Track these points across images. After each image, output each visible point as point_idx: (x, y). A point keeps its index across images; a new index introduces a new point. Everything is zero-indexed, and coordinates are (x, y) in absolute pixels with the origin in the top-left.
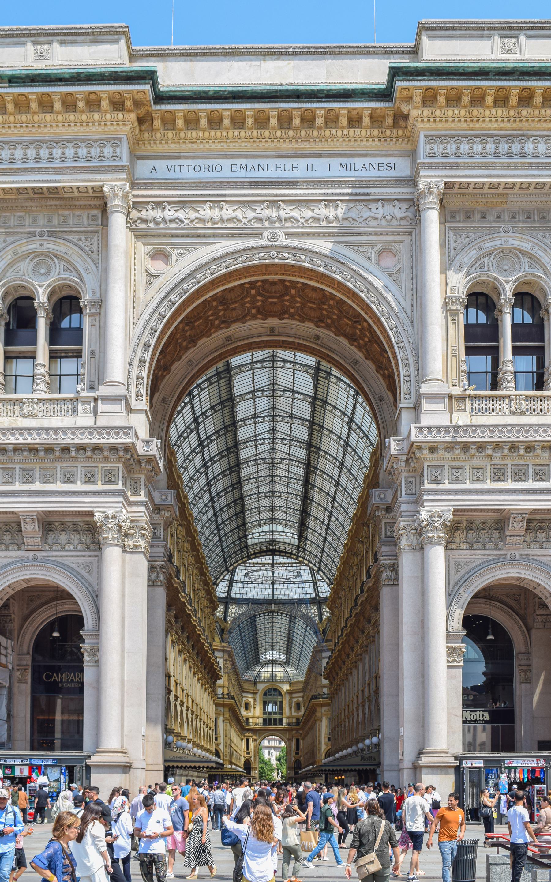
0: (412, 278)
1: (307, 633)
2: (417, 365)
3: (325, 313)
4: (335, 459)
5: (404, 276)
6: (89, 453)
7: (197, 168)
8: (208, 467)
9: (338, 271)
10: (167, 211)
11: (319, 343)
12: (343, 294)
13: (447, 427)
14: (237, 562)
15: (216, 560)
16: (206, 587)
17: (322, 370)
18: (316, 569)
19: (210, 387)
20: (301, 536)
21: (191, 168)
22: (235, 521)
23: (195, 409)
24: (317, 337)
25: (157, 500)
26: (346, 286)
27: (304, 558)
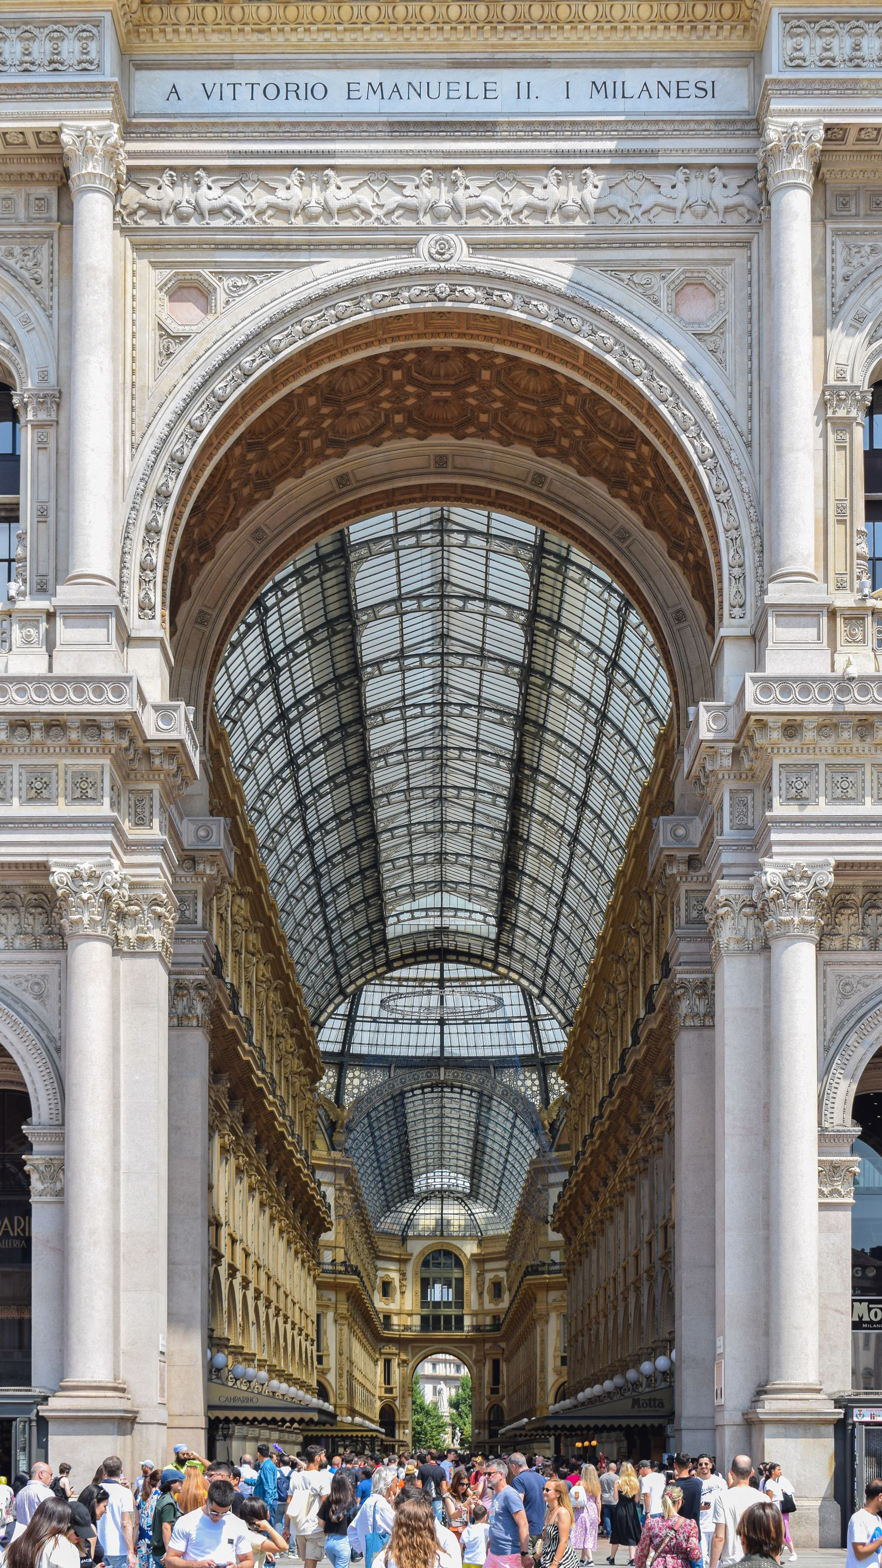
0: (750, 346)
1: (516, 1132)
2: (758, 541)
3: (558, 424)
4: (578, 749)
5: (731, 341)
6: (37, 736)
7: (271, 91)
8: (299, 768)
9: (586, 328)
10: (204, 189)
11: (544, 490)
13: (823, 679)
14: (363, 975)
15: (317, 971)
17: (550, 553)
18: (536, 991)
19: (303, 590)
20: (504, 921)
21: (258, 90)
22: (359, 888)
23: (271, 638)
24: (539, 479)
26: (603, 363)
27: (509, 968)
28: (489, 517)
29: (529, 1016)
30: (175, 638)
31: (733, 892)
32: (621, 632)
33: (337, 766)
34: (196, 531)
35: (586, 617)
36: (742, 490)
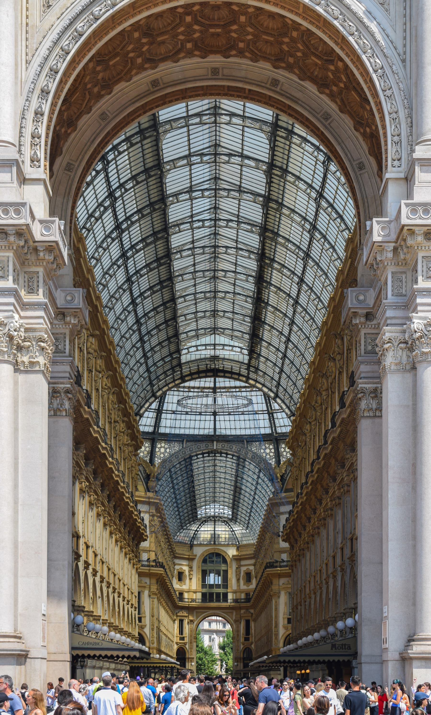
2: (409, 120)
3: (287, 49)
4: (299, 247)
8: (128, 258)
12: (311, 23)
14: (167, 385)
15: (139, 382)
16: (126, 419)
17: (282, 127)
18: (272, 395)
19: (130, 150)
22: (164, 332)
23: (111, 179)
24: (275, 82)
25: (60, 302)
26: (314, 12)
27: (256, 381)
28: (244, 106)
29: (268, 410)
30: (53, 179)
31: (394, 334)
32: (325, 176)
33: (151, 257)
34: (66, 114)
35: (303, 167)
36: (400, 89)
